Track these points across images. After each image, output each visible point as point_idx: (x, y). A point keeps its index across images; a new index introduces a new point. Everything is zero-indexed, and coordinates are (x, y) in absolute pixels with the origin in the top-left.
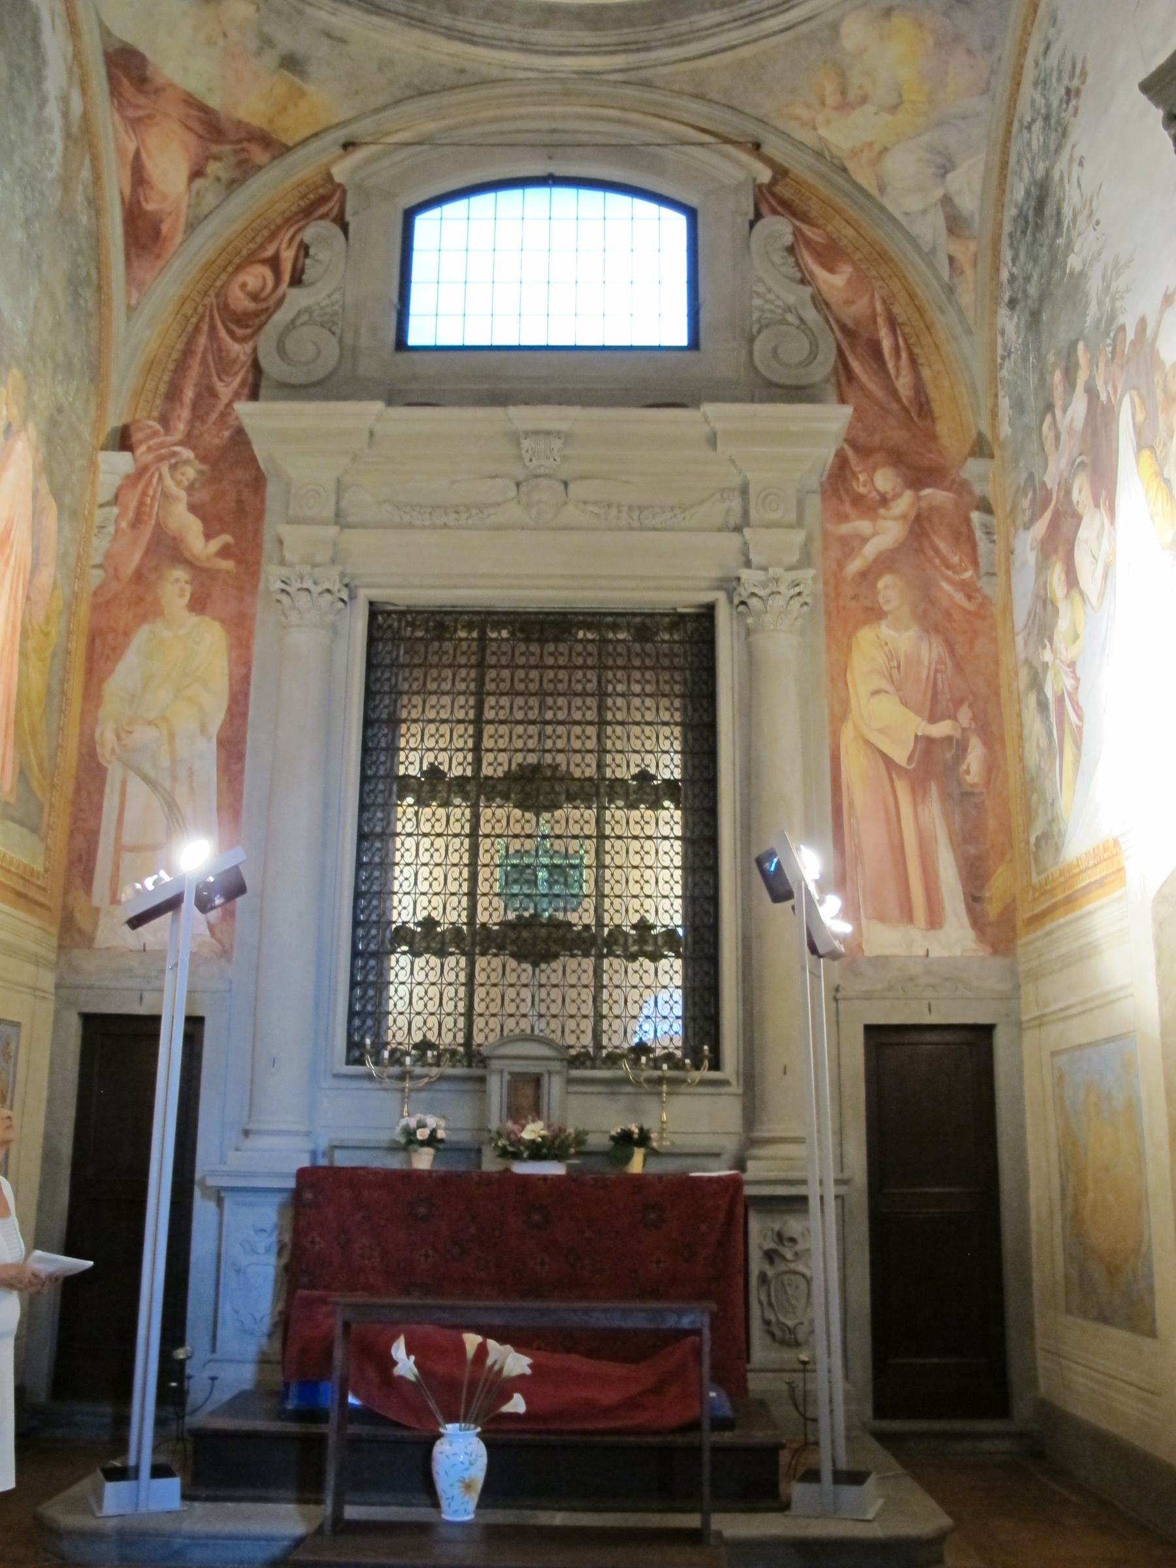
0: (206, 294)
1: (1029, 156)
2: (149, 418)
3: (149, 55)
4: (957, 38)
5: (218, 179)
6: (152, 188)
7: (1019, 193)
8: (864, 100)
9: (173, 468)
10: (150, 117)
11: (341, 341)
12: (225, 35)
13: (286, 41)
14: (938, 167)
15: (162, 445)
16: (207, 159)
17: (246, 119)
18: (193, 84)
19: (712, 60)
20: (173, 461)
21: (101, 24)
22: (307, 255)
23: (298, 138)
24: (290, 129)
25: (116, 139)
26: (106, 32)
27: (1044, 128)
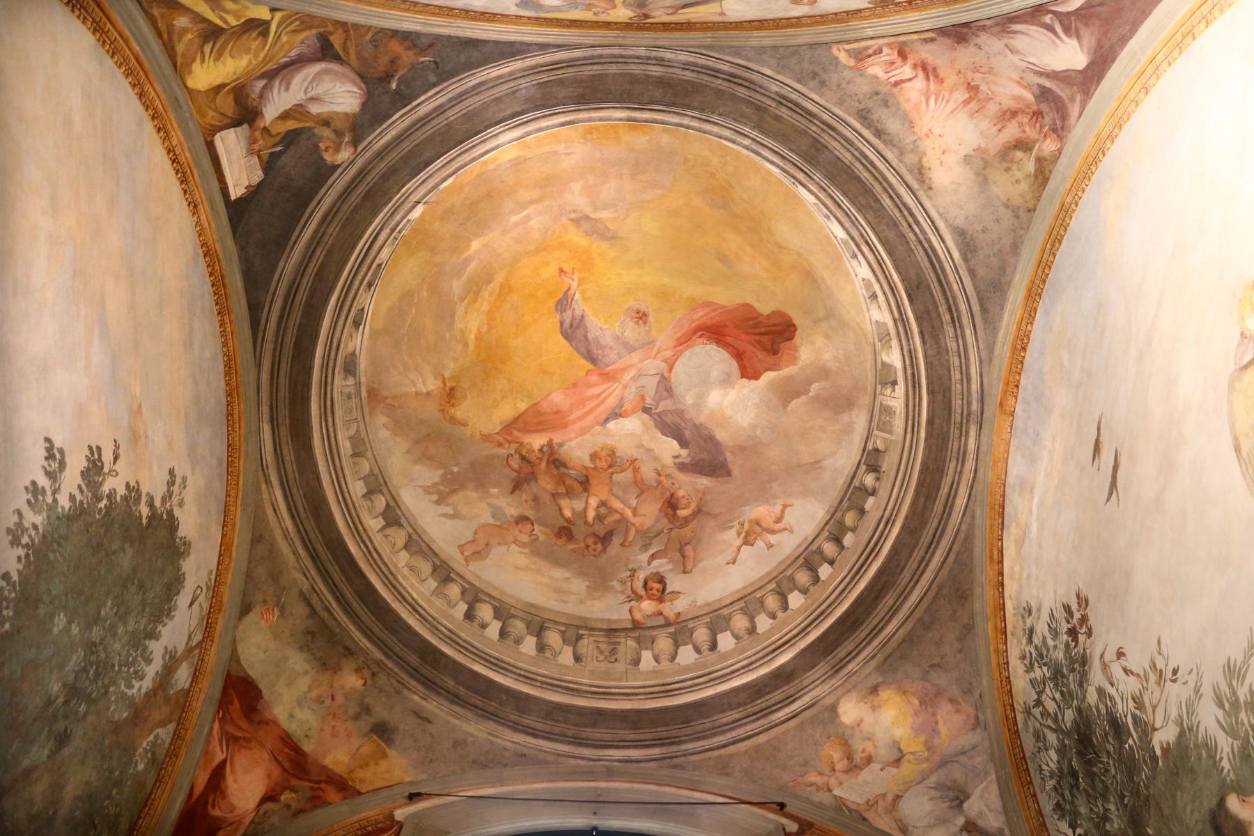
1: (1050, 722)
3: (265, 693)
4: (939, 694)
7: (1052, 759)
8: (869, 760)
10: (247, 740)
13: (380, 712)
14: (951, 801)
16: (285, 789)
17: (330, 767)
18: (292, 727)
19: (732, 749)
21: (234, 650)
23: (370, 788)
24: (368, 778)
25: (208, 742)
26: (234, 657)
27: (1056, 685)
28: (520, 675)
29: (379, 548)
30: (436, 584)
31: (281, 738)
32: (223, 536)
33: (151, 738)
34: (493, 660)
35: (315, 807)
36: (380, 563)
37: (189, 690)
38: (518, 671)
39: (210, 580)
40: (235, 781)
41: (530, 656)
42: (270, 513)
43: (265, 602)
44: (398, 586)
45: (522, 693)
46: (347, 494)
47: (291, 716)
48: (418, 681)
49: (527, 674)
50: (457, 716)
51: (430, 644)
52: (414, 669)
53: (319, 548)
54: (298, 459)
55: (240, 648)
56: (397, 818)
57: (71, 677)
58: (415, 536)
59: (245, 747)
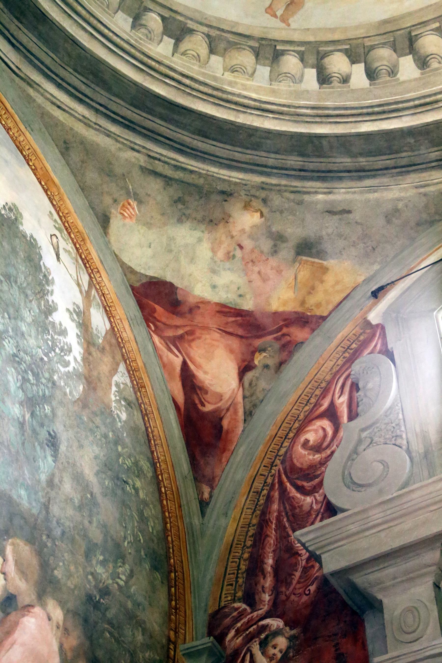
0: (272, 465)
2: (234, 601)
5: (266, 366)
6: (206, 392)
9: (263, 644)
10: (191, 333)
11: (408, 451)
12: (241, 247)
15: (248, 625)
17: (281, 309)
20: (263, 636)
21: (123, 265)
22: (358, 389)
23: (330, 307)
28: (416, 107)
29: (186, 72)
30: (269, 69)
31: (218, 312)
32: (34, 171)
33: (114, 389)
34: (376, 109)
35: (291, 354)
36: (196, 86)
37: (112, 328)
38: (411, 104)
39: (55, 221)
40: (206, 373)
41: (416, 80)
42: (57, 113)
43: (115, 201)
44: (230, 97)
45: (428, 124)
46: (115, 38)
47: (214, 287)
48: (312, 179)
49: (422, 101)
50: (372, 189)
51: (301, 135)
52: (300, 170)
53: (128, 114)
54: (40, 36)
55: (125, 259)
56: (374, 322)
57: (21, 394)
58: (214, 33)
59: (193, 340)
